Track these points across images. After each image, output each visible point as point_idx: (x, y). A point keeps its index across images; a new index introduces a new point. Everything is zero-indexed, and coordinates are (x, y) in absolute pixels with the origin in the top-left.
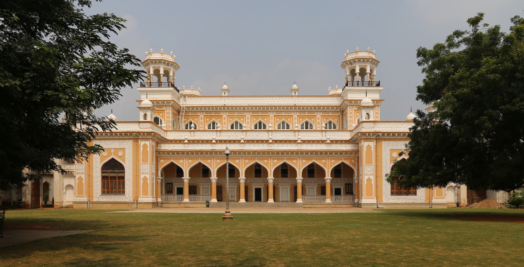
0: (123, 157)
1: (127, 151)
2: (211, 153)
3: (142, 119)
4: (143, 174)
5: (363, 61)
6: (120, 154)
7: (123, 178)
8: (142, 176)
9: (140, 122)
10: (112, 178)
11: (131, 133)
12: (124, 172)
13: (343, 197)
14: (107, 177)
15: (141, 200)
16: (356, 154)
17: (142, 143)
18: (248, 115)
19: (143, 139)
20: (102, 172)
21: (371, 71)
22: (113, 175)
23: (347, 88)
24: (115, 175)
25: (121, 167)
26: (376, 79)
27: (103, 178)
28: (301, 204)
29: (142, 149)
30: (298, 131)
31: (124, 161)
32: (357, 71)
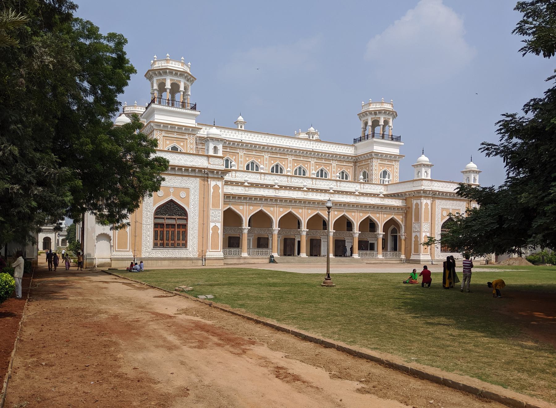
0: (187, 199)
1: (192, 192)
2: (276, 200)
3: (211, 153)
4: (213, 222)
5: (176, 74)
6: (183, 195)
7: (185, 226)
8: (212, 225)
9: (209, 157)
10: (168, 225)
11: (200, 170)
12: (187, 219)
13: (388, 253)
14: (162, 225)
15: (209, 255)
16: (406, 211)
17: (213, 183)
18: (266, 156)
19: (214, 178)
20: (155, 218)
21: (186, 88)
22: (172, 224)
23: (153, 105)
24: (173, 222)
25: (183, 212)
26: (190, 100)
27: (156, 225)
28: (357, 259)
29: (212, 190)
30: (291, 176)
31: (188, 204)
32: (168, 86)
